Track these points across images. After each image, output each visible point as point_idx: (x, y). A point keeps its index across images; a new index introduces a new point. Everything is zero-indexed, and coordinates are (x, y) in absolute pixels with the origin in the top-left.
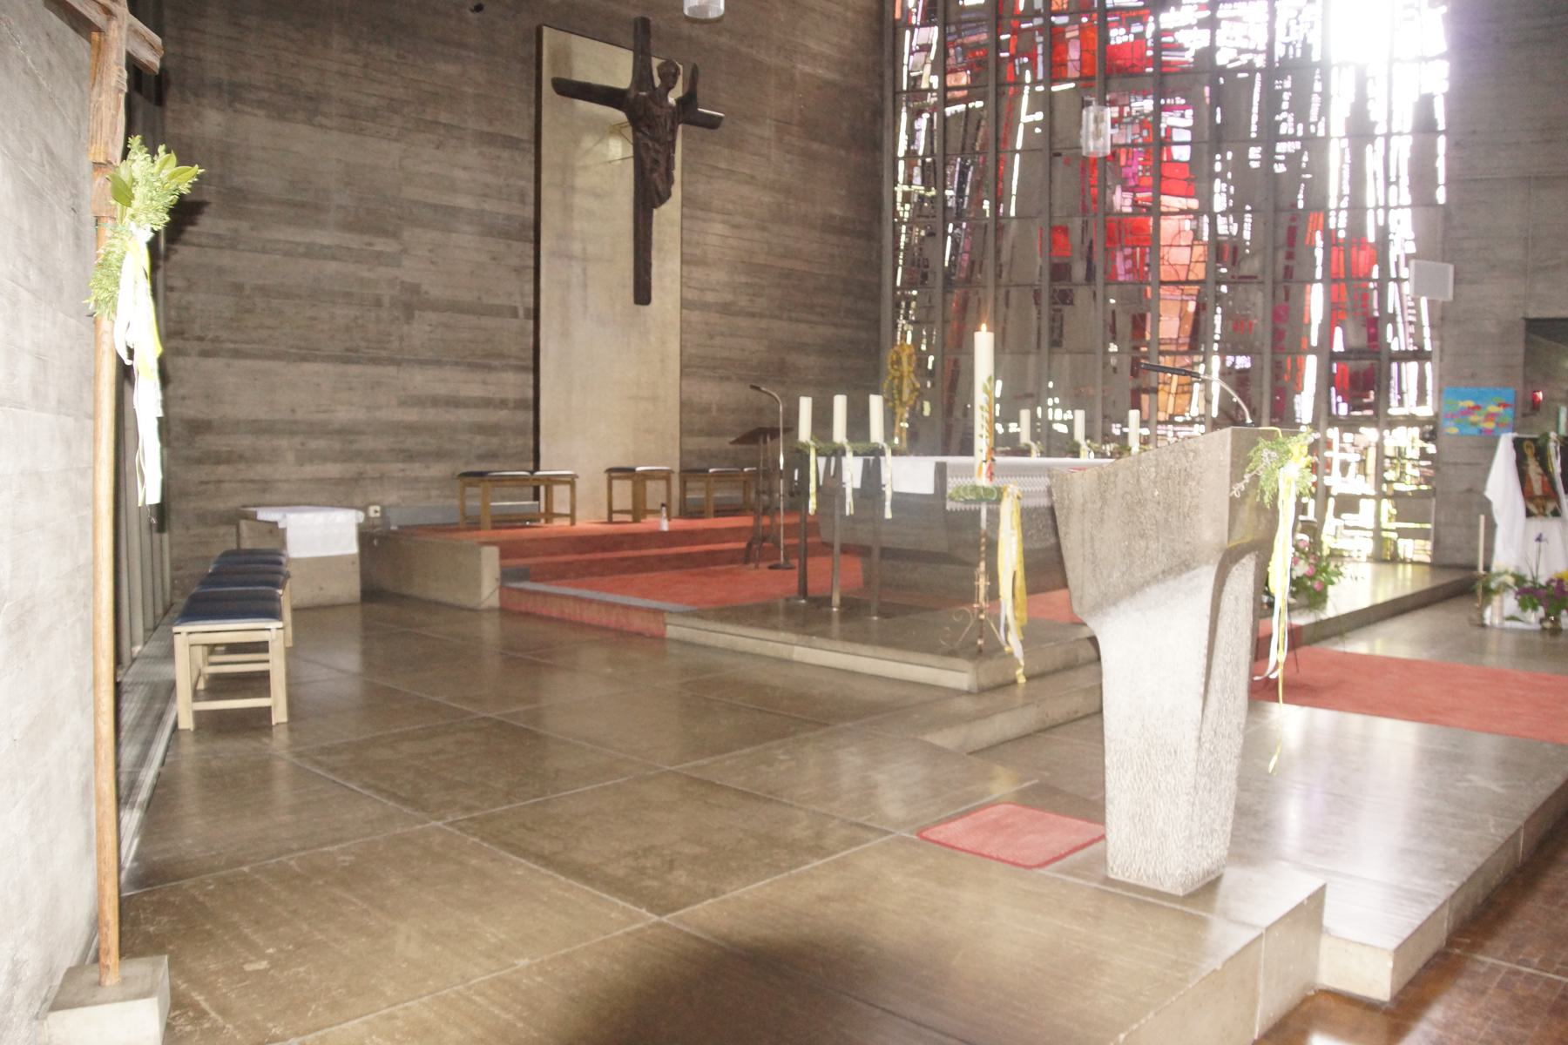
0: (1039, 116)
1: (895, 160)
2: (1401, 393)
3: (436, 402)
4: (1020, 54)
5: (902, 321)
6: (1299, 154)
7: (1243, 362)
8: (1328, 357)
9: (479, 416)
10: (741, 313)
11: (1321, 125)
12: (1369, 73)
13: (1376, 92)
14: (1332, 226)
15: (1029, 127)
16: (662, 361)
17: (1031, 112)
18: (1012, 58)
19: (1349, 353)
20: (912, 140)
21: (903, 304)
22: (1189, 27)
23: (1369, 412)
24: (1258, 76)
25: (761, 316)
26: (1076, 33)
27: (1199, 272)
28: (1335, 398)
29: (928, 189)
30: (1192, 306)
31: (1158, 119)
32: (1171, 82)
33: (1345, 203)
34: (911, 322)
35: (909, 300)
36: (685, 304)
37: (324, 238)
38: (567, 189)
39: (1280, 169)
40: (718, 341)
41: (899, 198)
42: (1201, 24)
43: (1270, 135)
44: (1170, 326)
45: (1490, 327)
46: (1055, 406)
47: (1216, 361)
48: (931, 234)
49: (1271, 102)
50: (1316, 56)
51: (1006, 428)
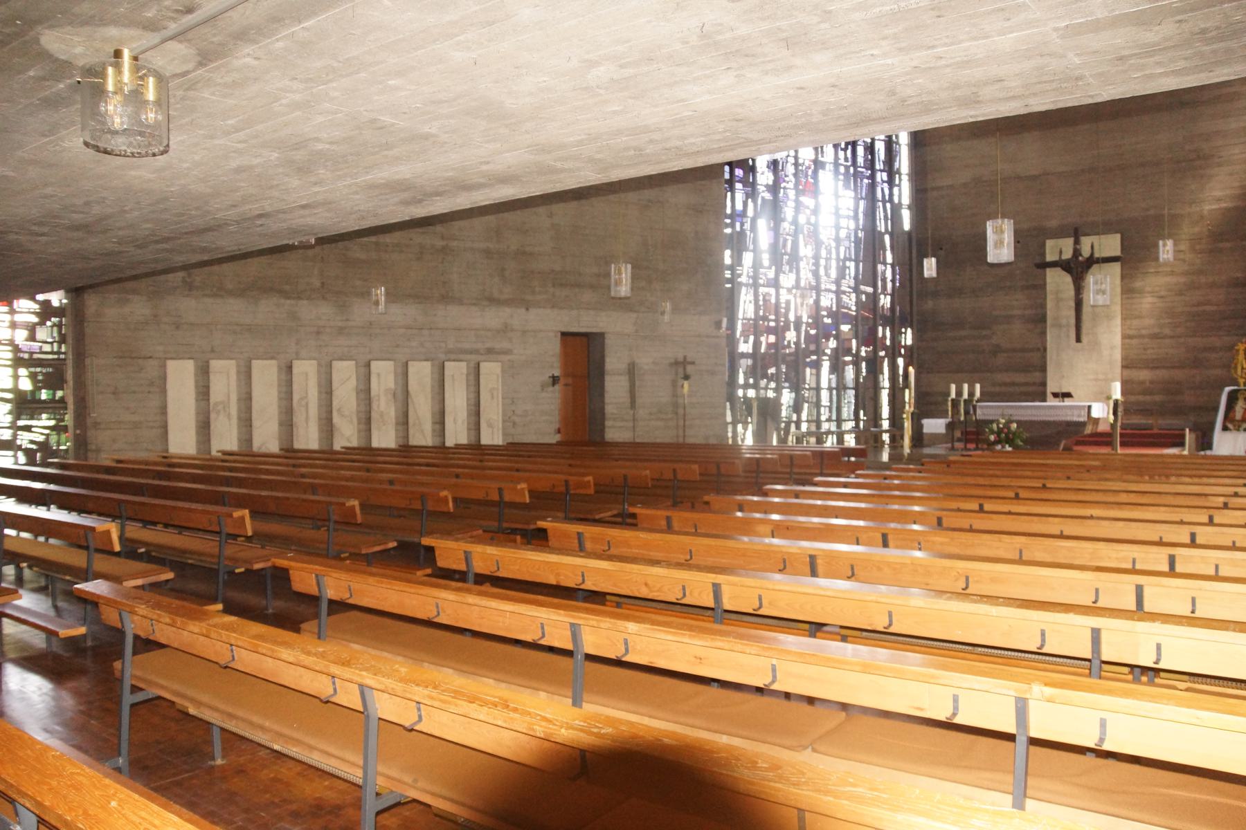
3: (1005, 384)
9: (1023, 389)
10: (1165, 337)
25: (1179, 337)
36: (1125, 337)
40: (1149, 352)
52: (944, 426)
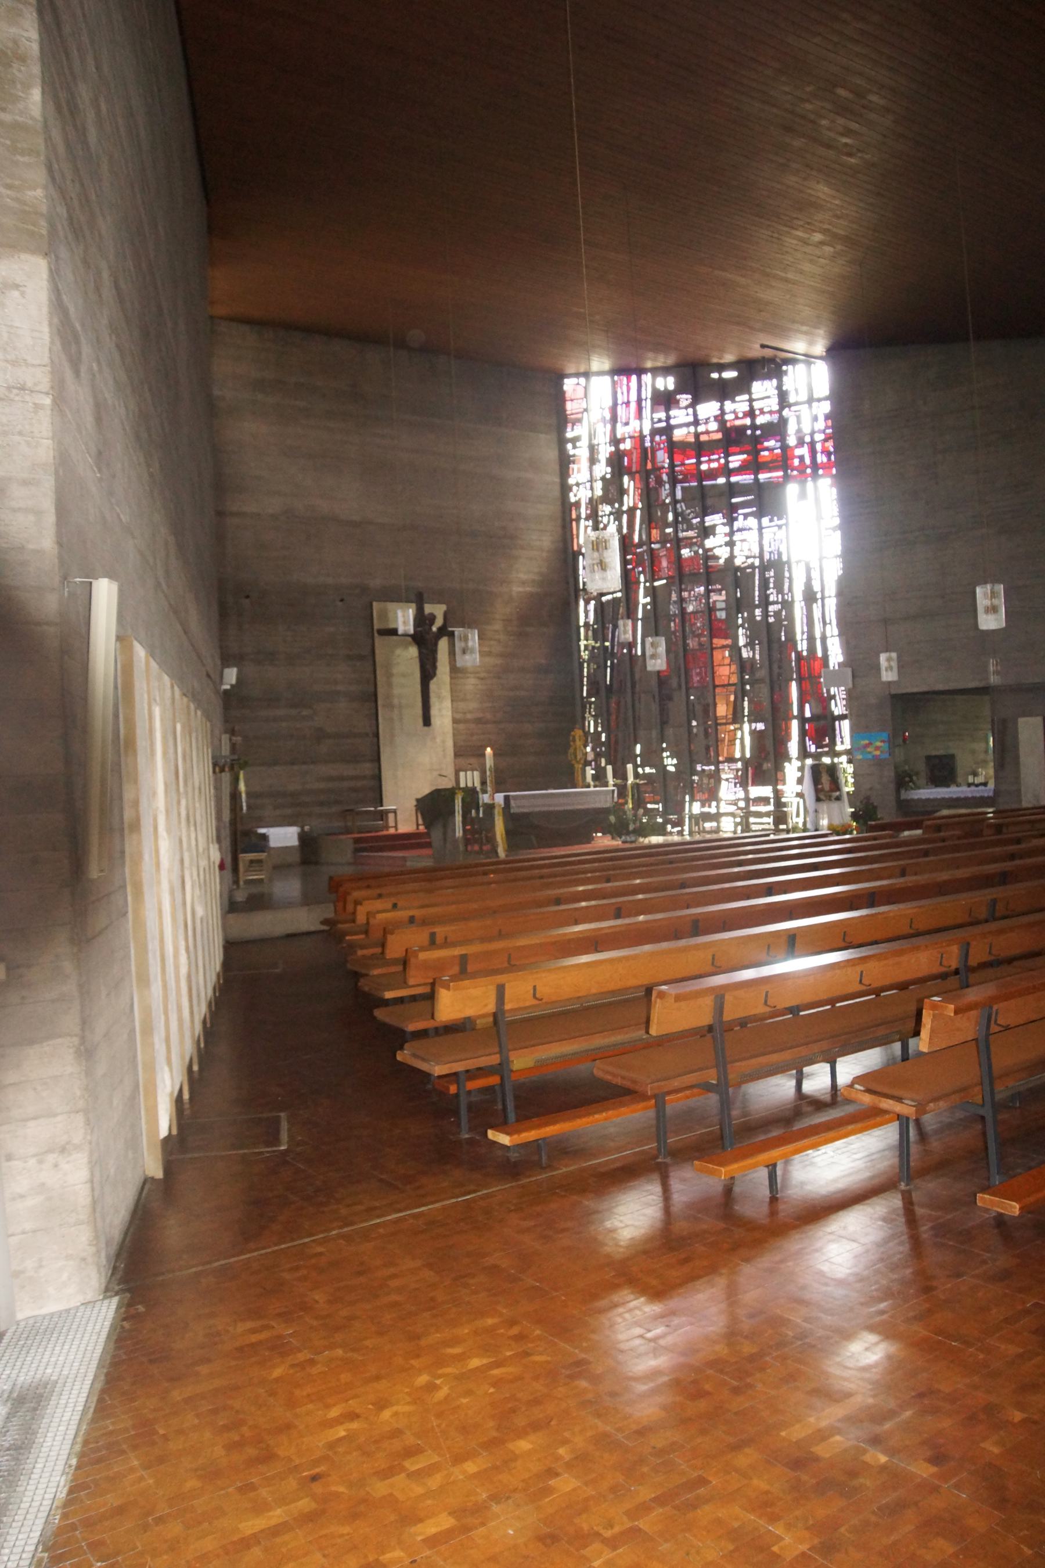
0: (648, 599)
1: (579, 627)
2: (841, 737)
4: (637, 566)
5: (587, 715)
6: (780, 611)
7: (760, 726)
8: (803, 720)
10: (486, 722)
11: (790, 594)
12: (811, 566)
13: (815, 575)
14: (799, 649)
15: (645, 606)
16: (444, 751)
17: (645, 597)
18: (634, 569)
19: (814, 718)
20: (587, 616)
21: (588, 706)
22: (721, 546)
23: (826, 749)
24: (757, 570)
26: (665, 553)
27: (734, 679)
28: (808, 743)
29: (596, 643)
30: (732, 698)
31: (708, 597)
32: (713, 577)
33: (805, 636)
34: (593, 716)
35: (591, 703)
36: (455, 721)
37: (280, 712)
38: (389, 675)
39: (771, 620)
40: (475, 738)
41: (582, 648)
42: (727, 544)
43: (765, 602)
44: (722, 710)
45: (873, 701)
46: (667, 757)
47: (746, 727)
48: (598, 667)
49: (765, 584)
50: (785, 558)
51: (644, 770)
52: (296, 837)
